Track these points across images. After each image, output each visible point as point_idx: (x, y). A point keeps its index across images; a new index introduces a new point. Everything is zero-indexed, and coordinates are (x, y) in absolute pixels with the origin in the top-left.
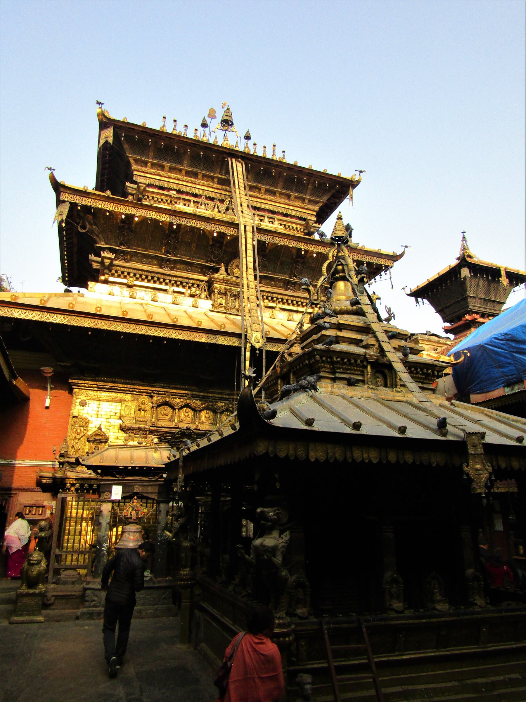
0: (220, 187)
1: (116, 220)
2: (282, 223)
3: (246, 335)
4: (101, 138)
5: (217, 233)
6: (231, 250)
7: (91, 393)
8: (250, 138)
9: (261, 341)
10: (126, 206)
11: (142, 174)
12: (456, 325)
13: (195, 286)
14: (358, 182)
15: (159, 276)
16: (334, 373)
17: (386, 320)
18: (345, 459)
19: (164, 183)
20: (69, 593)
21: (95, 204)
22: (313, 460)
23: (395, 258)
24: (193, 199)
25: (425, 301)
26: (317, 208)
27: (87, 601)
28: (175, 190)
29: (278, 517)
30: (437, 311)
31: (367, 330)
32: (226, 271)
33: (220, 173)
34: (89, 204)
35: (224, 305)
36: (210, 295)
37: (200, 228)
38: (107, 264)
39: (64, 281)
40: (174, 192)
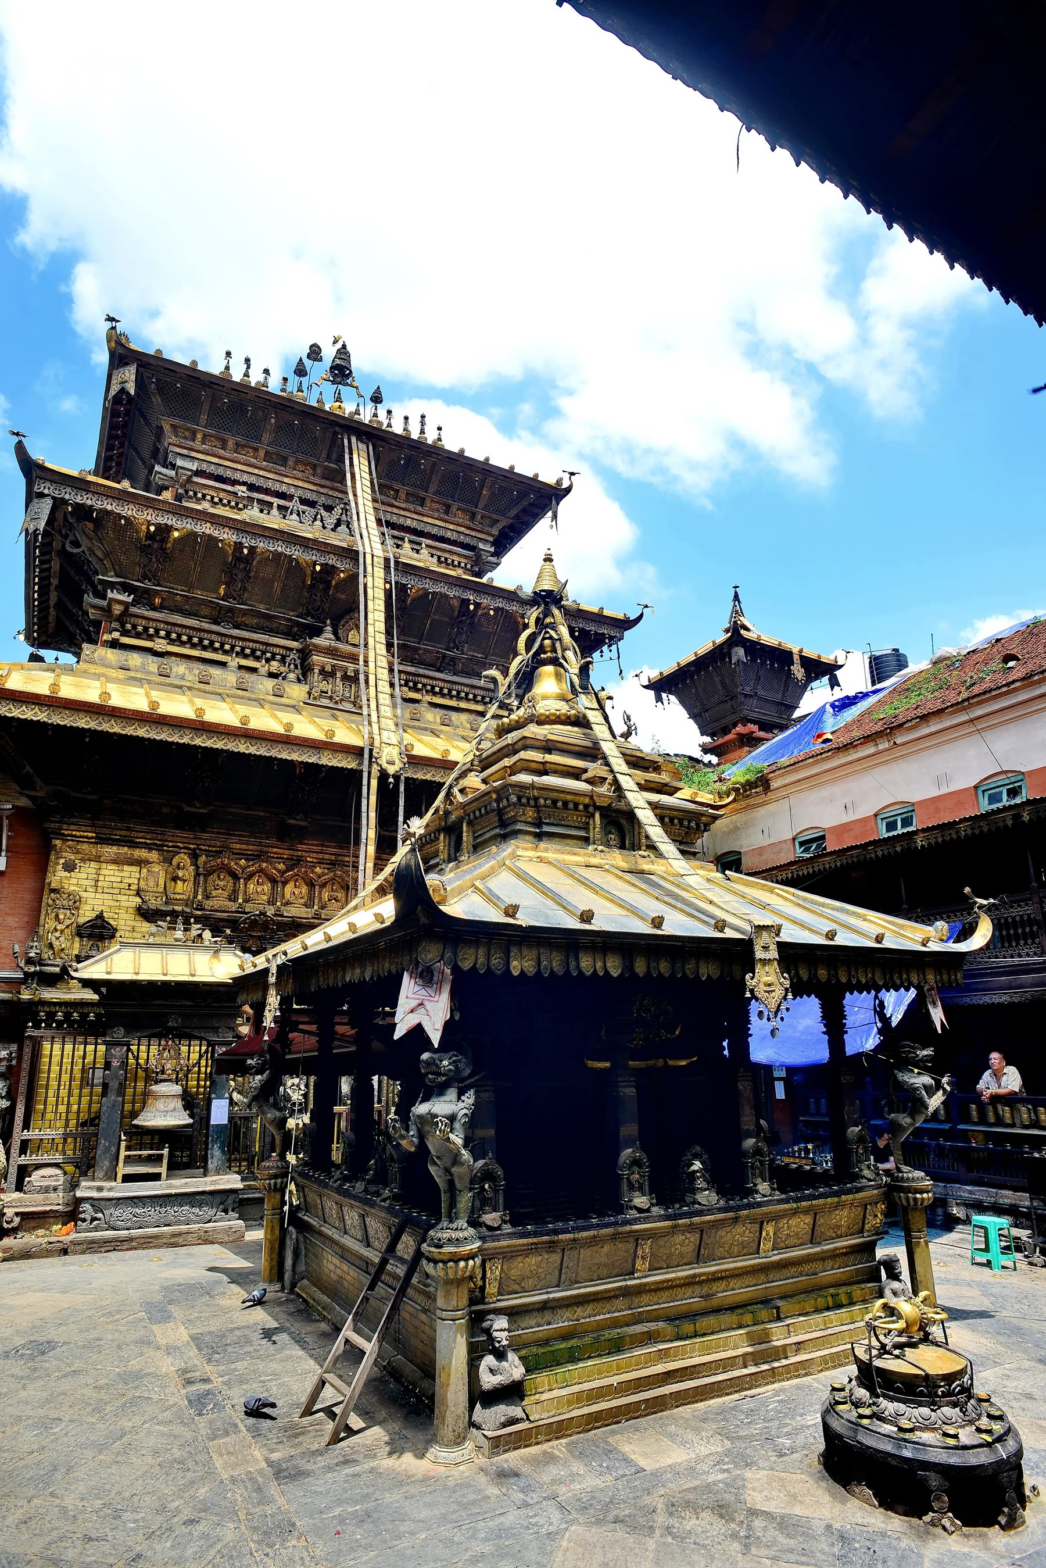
0: (328, 483)
1: (137, 532)
2: (434, 552)
3: (371, 751)
4: (113, 382)
5: (321, 565)
6: (343, 597)
7: (85, 846)
8: (381, 402)
9: (397, 761)
10: (157, 509)
11: (185, 452)
12: (721, 741)
13: (278, 657)
14: (568, 490)
15: (214, 637)
16: (539, 824)
17: (622, 736)
18: (568, 972)
19: (225, 472)
20: (48, 1208)
21: (99, 503)
22: (516, 973)
23: (627, 624)
24: (276, 501)
25: (672, 698)
26: (495, 532)
27: (84, 1220)
28: (244, 484)
29: (456, 1067)
30: (693, 716)
31: (593, 753)
32: (335, 633)
33: (328, 458)
34: (89, 502)
35: (330, 693)
36: (304, 675)
37: (291, 556)
38: (117, 612)
39: (28, 638)
40: (244, 488)
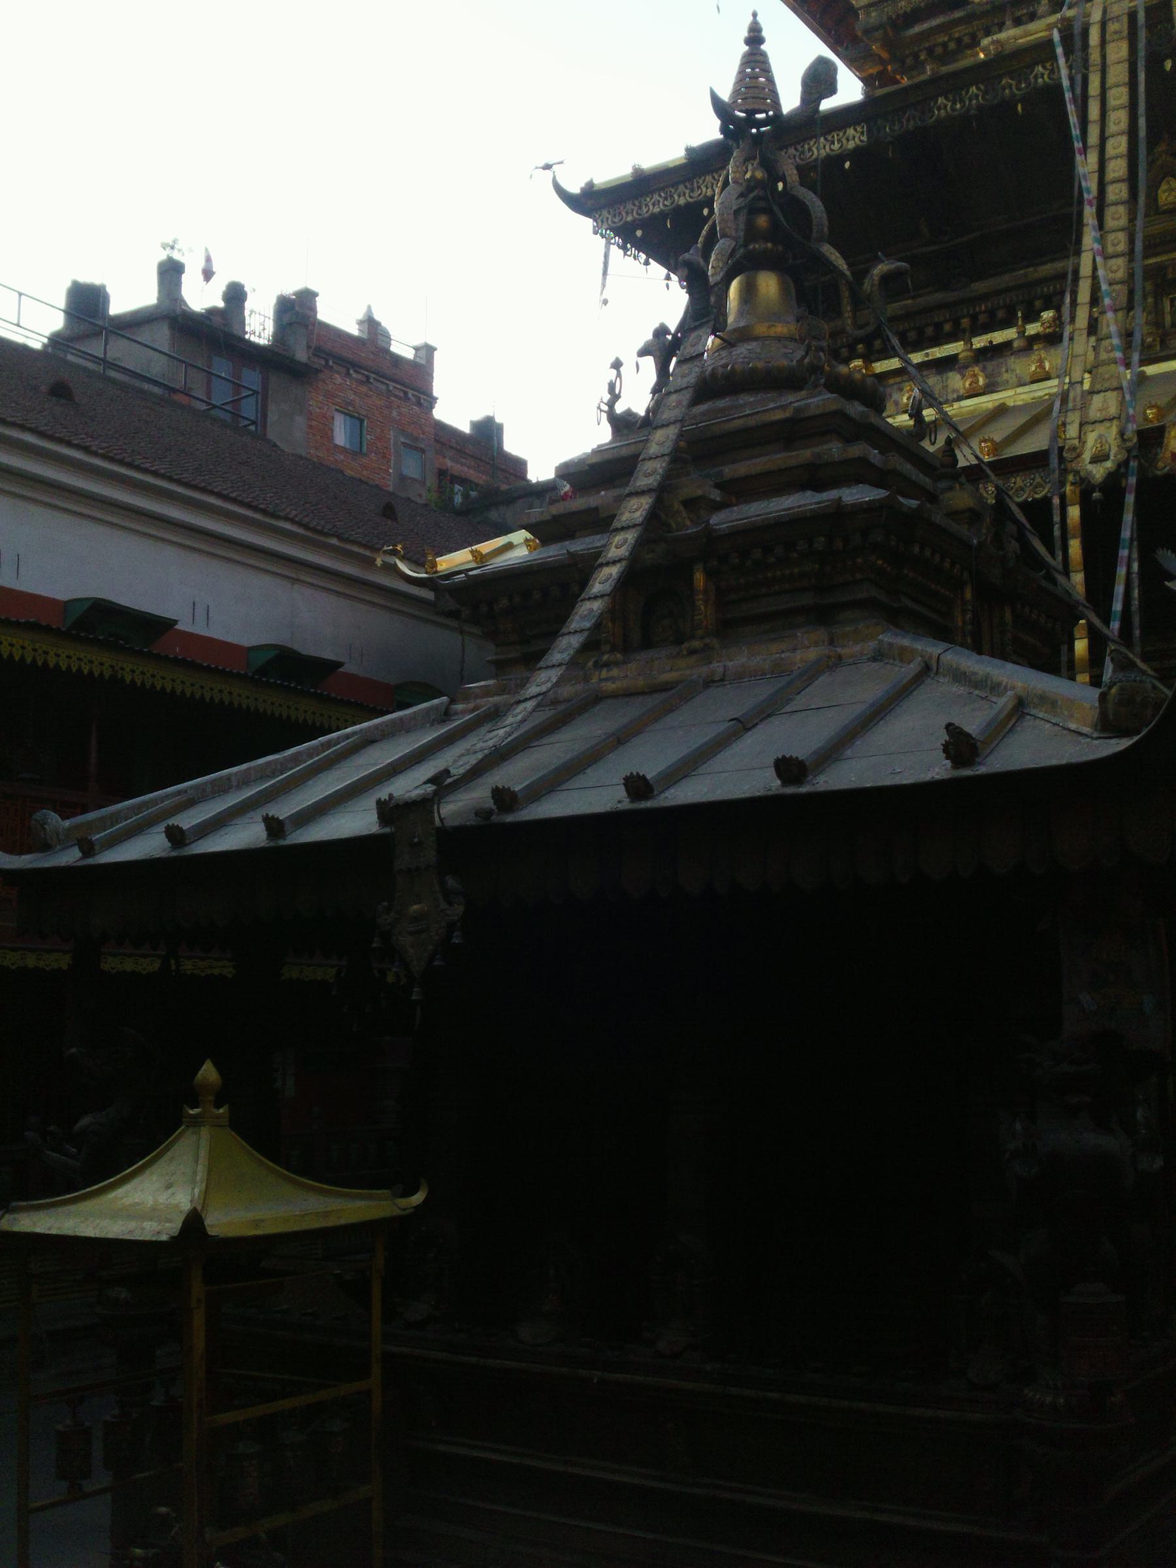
3: (1061, 449)
